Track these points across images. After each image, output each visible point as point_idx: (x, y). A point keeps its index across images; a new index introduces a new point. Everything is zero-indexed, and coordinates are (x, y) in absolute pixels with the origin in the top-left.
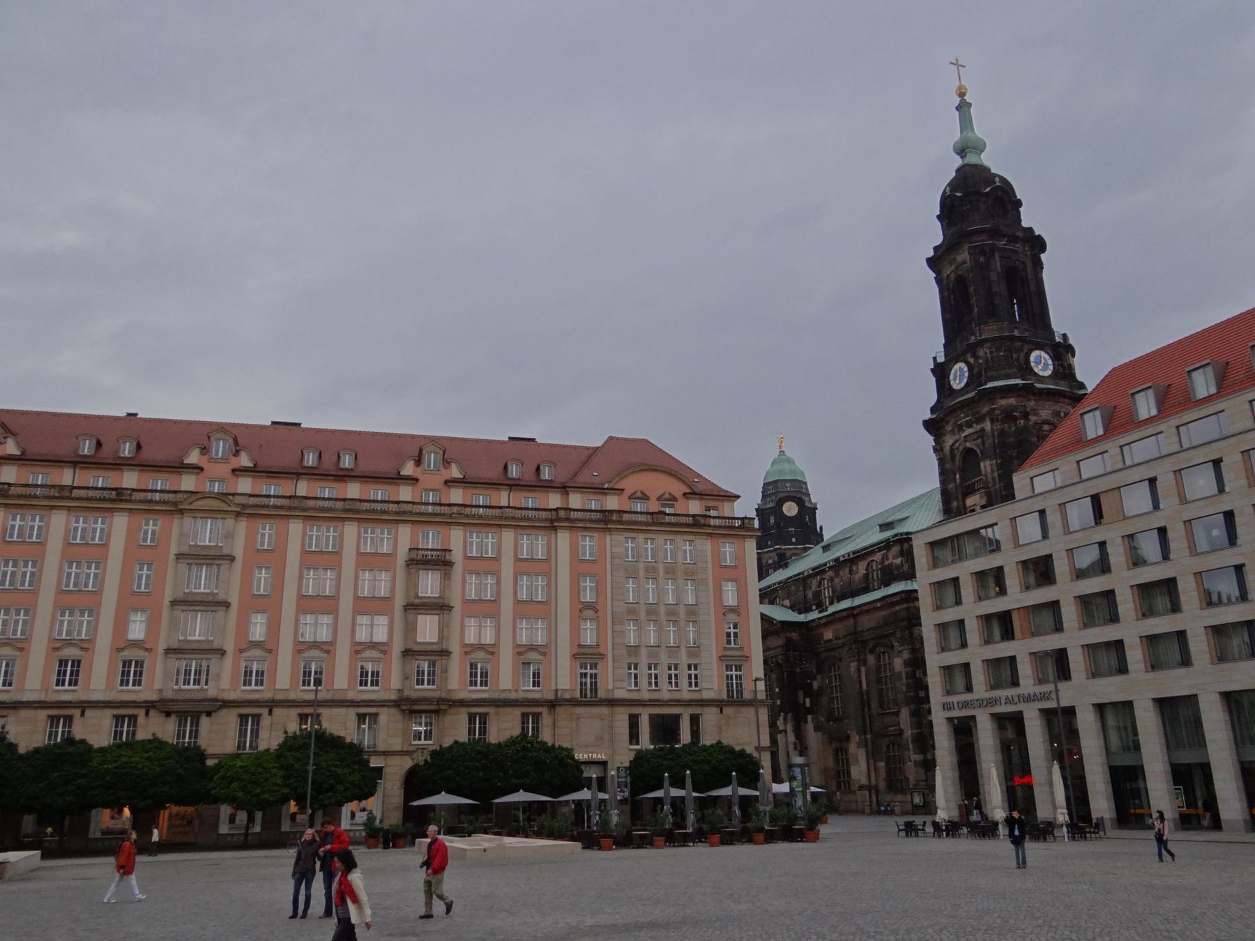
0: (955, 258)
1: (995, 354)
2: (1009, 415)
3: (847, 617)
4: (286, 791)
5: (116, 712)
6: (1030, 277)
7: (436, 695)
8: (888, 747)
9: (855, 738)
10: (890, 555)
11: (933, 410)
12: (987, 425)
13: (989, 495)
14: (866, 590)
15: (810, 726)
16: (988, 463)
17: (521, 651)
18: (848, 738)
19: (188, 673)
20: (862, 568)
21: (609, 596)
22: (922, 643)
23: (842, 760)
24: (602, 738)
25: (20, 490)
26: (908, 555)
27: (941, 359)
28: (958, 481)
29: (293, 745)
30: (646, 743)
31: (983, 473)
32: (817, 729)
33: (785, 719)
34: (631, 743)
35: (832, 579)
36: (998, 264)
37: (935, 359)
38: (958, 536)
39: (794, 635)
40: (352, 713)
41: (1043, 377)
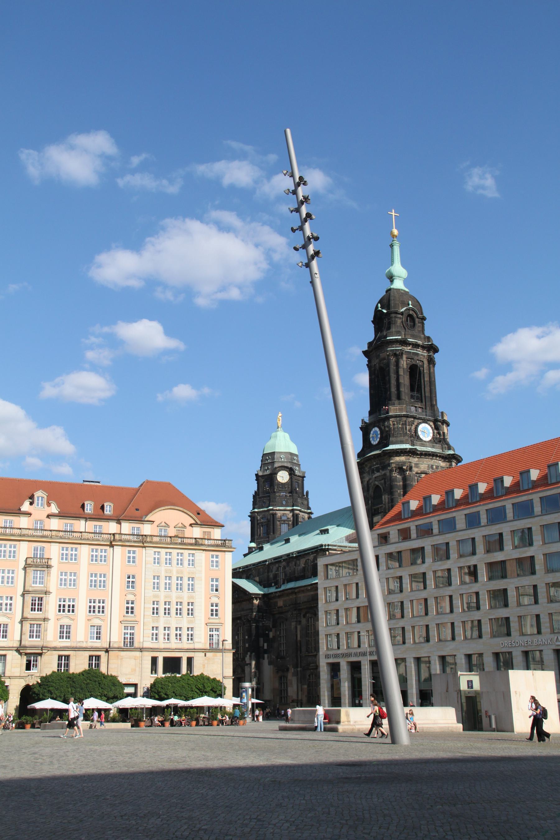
0: (379, 355)
1: (396, 426)
6: (425, 371)
8: (309, 676)
9: (292, 670)
15: (266, 662)
16: (387, 496)
18: (288, 670)
23: (284, 683)
27: (367, 420)
28: (370, 505)
30: (160, 674)
31: (384, 503)
32: (270, 663)
34: (152, 673)
36: (405, 363)
41: (425, 441)
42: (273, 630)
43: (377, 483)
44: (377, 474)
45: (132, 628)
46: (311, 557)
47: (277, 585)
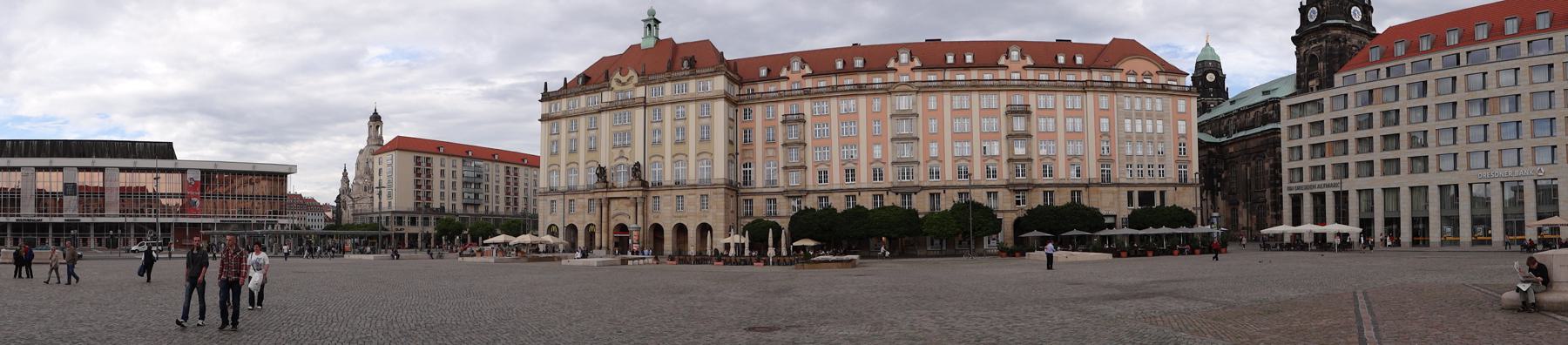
2: (1336, 39)
3: (1243, 140)
4: (958, 230)
5: (875, 193)
7: (1027, 181)
10: (1267, 109)
11: (1297, 31)
12: (1324, 44)
13: (1320, 80)
14: (1253, 127)
17: (1070, 158)
19: (903, 174)
20: (1252, 114)
21: (1116, 128)
22: (1281, 156)
24: (1113, 203)
25: (815, 90)
26: (1278, 110)
29: (957, 207)
30: (1136, 205)
33: (1207, 193)
35: (1235, 120)
37: (1301, 3)
38: (1304, 103)
39: (1213, 149)
40: (984, 191)
42: (1225, 172)
43: (1313, 53)
44: (1315, 45)
45: (1108, 166)
46: (1261, 109)
47: (1228, 135)
